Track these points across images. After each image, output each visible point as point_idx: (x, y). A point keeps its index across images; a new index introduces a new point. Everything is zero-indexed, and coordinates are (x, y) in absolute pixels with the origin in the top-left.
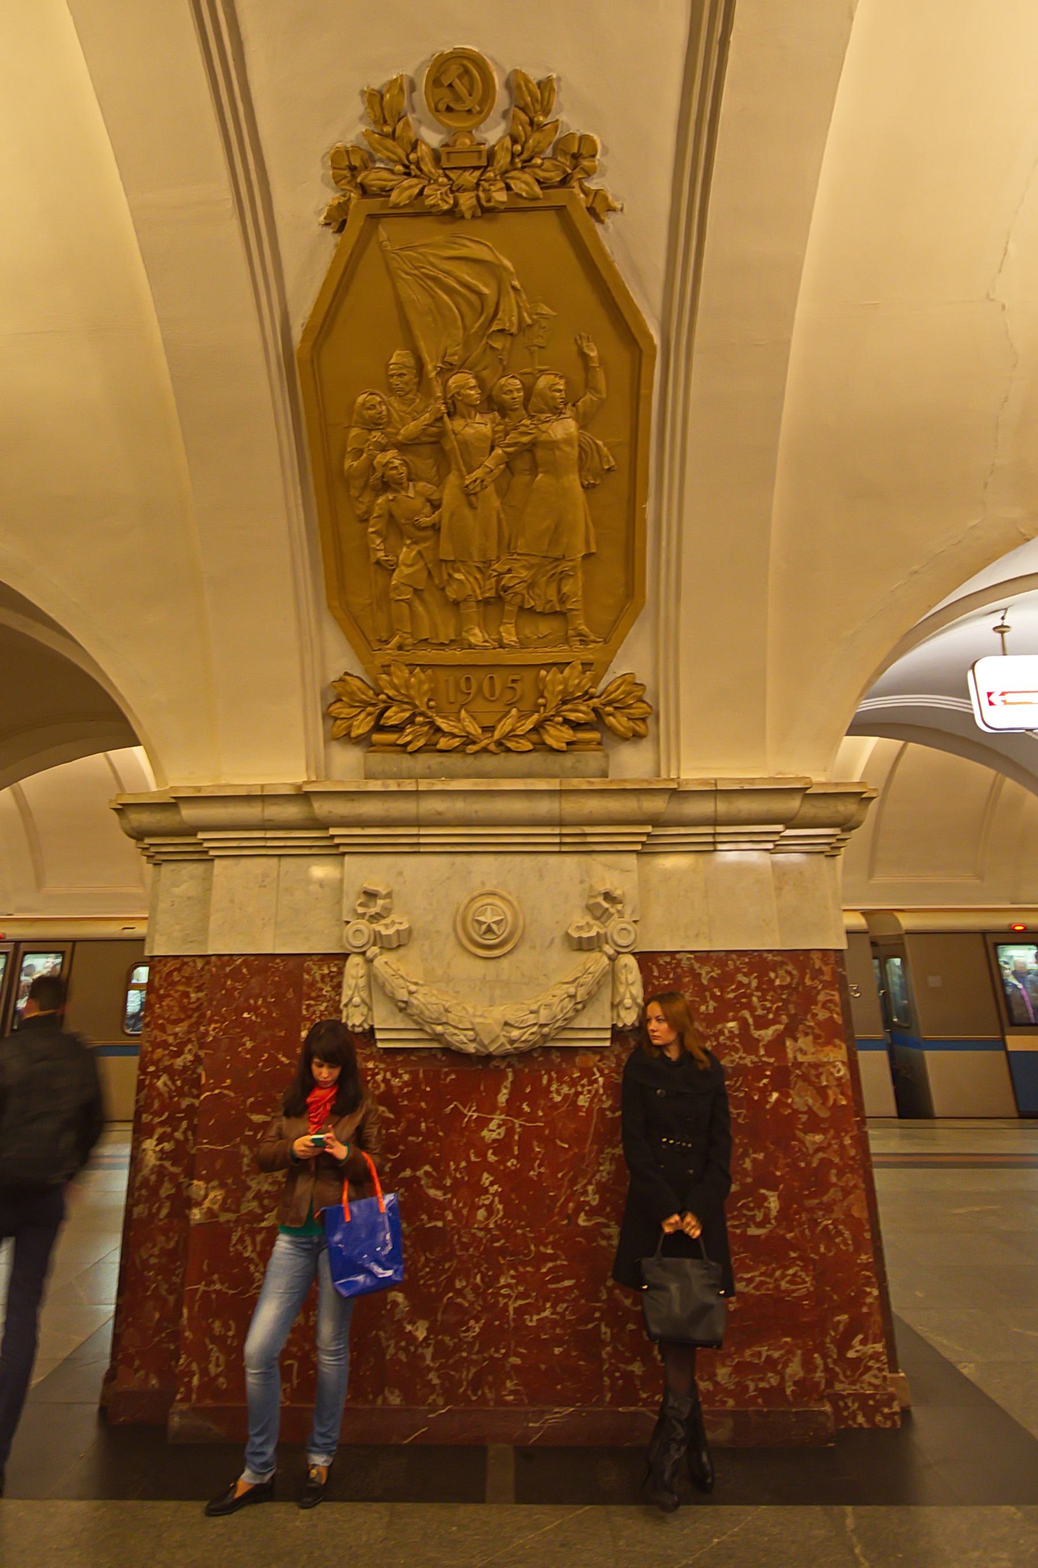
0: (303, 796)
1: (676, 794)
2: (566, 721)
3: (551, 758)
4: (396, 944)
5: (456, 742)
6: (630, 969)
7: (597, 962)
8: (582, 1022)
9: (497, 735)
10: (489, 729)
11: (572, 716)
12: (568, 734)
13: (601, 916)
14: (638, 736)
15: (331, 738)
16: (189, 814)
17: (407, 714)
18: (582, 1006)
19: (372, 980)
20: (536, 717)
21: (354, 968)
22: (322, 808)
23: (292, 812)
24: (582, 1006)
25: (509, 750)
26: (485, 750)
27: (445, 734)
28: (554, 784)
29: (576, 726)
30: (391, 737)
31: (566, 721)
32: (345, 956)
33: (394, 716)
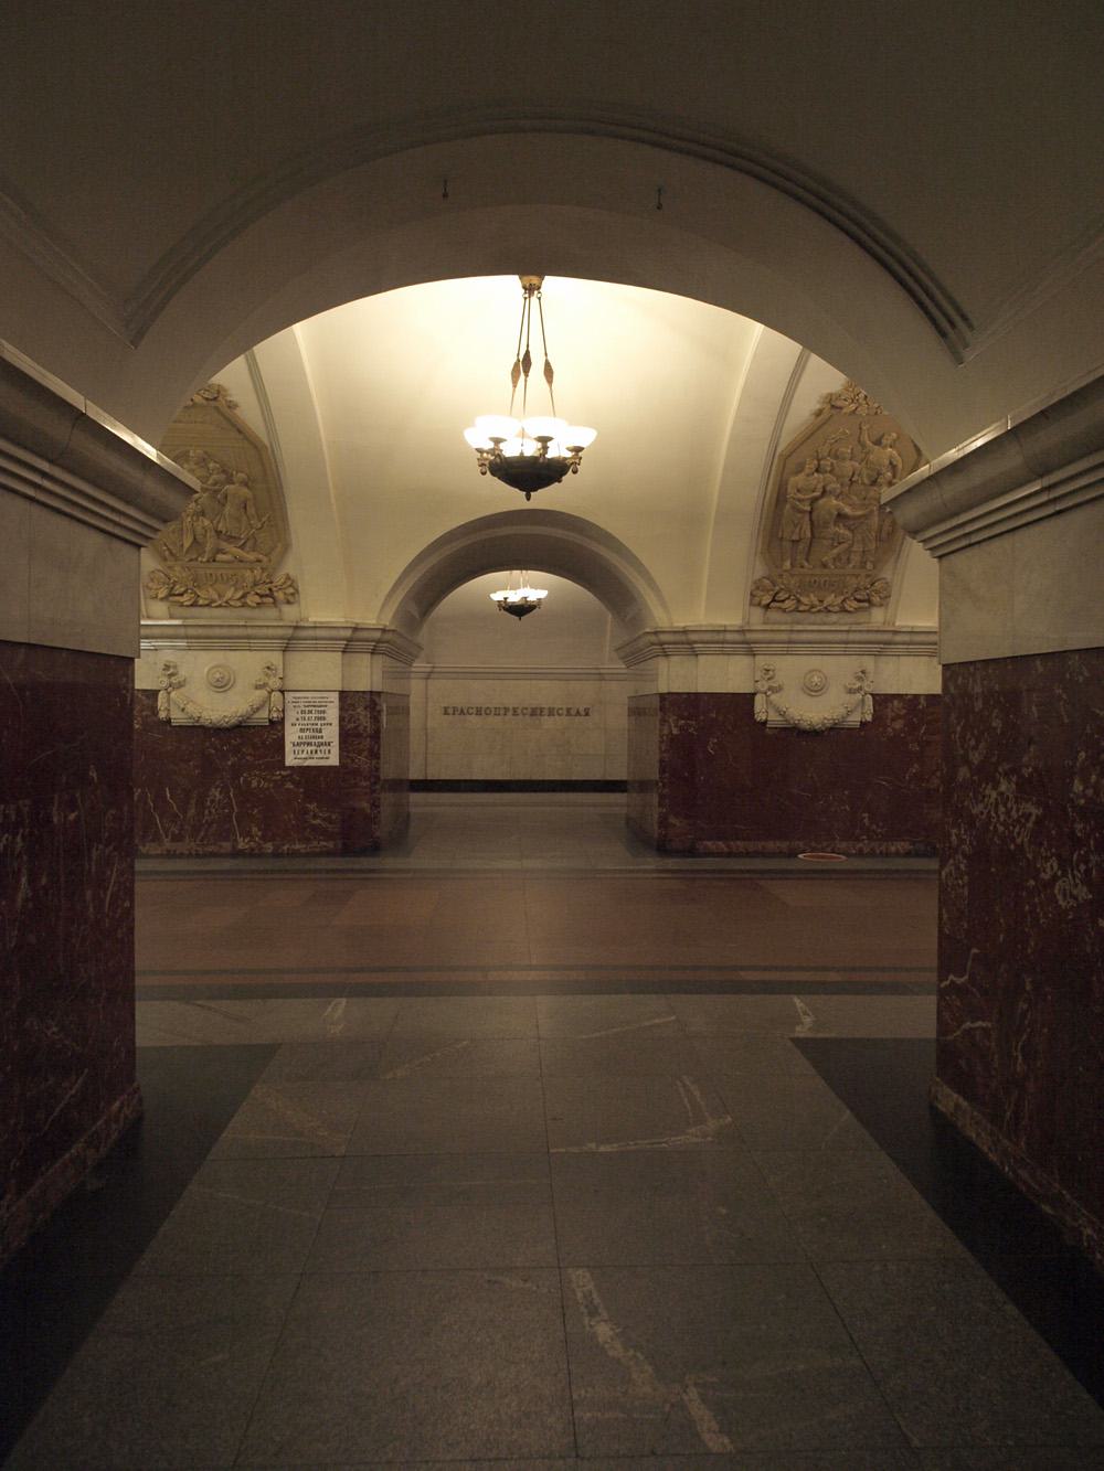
0: (742, 631)
1: (895, 632)
2: (855, 599)
3: (849, 615)
4: (778, 689)
5: (807, 608)
6: (869, 700)
7: (859, 696)
8: (849, 719)
9: (825, 604)
10: (821, 601)
11: (858, 597)
12: (855, 604)
13: (860, 679)
14: (881, 605)
15: (751, 604)
16: (693, 637)
17: (787, 596)
18: (849, 713)
19: (769, 702)
20: (842, 598)
21: (758, 698)
22: (749, 636)
23: (737, 637)
24: (849, 713)
25: (830, 611)
26: (819, 611)
27: (803, 604)
28: (846, 628)
29: (859, 601)
30: (778, 604)
31: (855, 599)
32: (754, 694)
33: (782, 596)
